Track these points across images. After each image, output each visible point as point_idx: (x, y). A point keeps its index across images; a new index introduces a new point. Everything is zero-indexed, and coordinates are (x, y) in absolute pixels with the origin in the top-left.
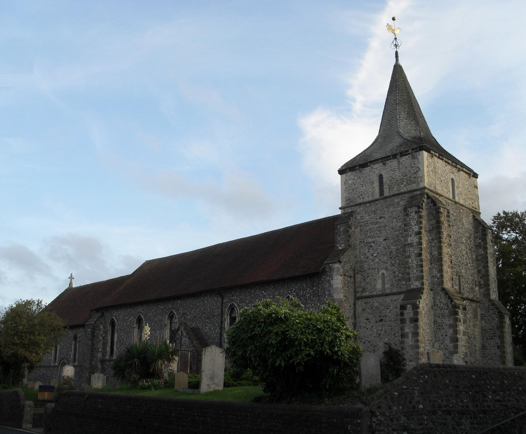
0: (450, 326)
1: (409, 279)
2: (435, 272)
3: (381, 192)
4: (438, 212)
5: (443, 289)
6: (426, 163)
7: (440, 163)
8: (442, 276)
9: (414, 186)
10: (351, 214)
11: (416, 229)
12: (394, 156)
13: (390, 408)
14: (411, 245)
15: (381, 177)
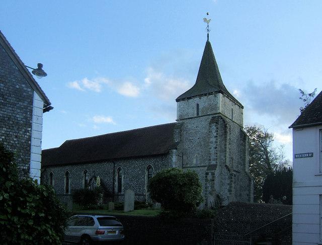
0: (228, 184)
1: (210, 160)
2: (222, 157)
3: (198, 114)
4: (226, 127)
5: (226, 166)
6: (221, 100)
7: (227, 100)
8: (226, 159)
9: (214, 112)
10: (182, 124)
11: (215, 134)
12: (205, 95)
13: (221, 219)
14: (212, 143)
15: (198, 105)
